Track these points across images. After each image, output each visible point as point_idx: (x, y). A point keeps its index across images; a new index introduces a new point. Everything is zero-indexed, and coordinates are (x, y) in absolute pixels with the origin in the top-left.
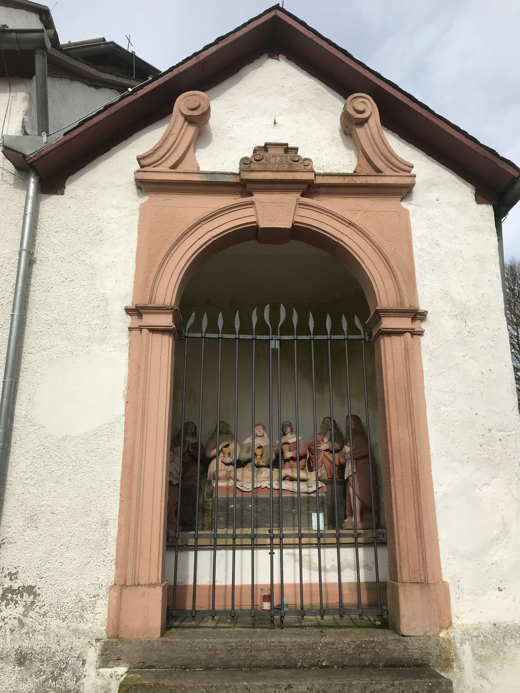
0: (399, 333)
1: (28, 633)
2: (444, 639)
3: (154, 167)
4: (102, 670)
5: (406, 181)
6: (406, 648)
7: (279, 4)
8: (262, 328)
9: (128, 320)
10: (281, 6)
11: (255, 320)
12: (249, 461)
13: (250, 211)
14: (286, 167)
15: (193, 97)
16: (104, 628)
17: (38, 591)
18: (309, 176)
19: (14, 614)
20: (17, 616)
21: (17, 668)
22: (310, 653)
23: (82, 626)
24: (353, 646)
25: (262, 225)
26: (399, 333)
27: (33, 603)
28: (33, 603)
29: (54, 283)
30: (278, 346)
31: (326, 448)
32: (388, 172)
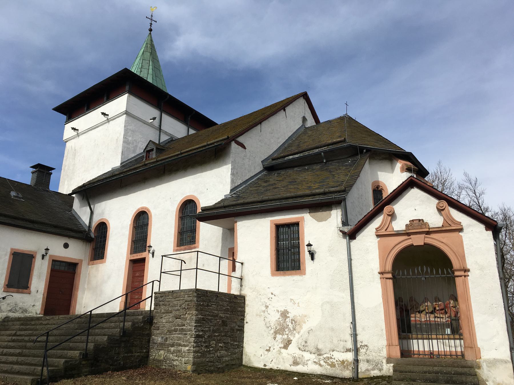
0: (461, 276)
1: (368, 356)
2: (478, 361)
4: (387, 365)
5: (460, 227)
6: (466, 363)
12: (423, 311)
13: (410, 240)
16: (386, 355)
17: (368, 346)
18: (428, 230)
19: (364, 351)
21: (367, 363)
23: (380, 355)
24: (452, 362)
26: (461, 276)
27: (368, 349)
28: (368, 349)
32: (454, 225)
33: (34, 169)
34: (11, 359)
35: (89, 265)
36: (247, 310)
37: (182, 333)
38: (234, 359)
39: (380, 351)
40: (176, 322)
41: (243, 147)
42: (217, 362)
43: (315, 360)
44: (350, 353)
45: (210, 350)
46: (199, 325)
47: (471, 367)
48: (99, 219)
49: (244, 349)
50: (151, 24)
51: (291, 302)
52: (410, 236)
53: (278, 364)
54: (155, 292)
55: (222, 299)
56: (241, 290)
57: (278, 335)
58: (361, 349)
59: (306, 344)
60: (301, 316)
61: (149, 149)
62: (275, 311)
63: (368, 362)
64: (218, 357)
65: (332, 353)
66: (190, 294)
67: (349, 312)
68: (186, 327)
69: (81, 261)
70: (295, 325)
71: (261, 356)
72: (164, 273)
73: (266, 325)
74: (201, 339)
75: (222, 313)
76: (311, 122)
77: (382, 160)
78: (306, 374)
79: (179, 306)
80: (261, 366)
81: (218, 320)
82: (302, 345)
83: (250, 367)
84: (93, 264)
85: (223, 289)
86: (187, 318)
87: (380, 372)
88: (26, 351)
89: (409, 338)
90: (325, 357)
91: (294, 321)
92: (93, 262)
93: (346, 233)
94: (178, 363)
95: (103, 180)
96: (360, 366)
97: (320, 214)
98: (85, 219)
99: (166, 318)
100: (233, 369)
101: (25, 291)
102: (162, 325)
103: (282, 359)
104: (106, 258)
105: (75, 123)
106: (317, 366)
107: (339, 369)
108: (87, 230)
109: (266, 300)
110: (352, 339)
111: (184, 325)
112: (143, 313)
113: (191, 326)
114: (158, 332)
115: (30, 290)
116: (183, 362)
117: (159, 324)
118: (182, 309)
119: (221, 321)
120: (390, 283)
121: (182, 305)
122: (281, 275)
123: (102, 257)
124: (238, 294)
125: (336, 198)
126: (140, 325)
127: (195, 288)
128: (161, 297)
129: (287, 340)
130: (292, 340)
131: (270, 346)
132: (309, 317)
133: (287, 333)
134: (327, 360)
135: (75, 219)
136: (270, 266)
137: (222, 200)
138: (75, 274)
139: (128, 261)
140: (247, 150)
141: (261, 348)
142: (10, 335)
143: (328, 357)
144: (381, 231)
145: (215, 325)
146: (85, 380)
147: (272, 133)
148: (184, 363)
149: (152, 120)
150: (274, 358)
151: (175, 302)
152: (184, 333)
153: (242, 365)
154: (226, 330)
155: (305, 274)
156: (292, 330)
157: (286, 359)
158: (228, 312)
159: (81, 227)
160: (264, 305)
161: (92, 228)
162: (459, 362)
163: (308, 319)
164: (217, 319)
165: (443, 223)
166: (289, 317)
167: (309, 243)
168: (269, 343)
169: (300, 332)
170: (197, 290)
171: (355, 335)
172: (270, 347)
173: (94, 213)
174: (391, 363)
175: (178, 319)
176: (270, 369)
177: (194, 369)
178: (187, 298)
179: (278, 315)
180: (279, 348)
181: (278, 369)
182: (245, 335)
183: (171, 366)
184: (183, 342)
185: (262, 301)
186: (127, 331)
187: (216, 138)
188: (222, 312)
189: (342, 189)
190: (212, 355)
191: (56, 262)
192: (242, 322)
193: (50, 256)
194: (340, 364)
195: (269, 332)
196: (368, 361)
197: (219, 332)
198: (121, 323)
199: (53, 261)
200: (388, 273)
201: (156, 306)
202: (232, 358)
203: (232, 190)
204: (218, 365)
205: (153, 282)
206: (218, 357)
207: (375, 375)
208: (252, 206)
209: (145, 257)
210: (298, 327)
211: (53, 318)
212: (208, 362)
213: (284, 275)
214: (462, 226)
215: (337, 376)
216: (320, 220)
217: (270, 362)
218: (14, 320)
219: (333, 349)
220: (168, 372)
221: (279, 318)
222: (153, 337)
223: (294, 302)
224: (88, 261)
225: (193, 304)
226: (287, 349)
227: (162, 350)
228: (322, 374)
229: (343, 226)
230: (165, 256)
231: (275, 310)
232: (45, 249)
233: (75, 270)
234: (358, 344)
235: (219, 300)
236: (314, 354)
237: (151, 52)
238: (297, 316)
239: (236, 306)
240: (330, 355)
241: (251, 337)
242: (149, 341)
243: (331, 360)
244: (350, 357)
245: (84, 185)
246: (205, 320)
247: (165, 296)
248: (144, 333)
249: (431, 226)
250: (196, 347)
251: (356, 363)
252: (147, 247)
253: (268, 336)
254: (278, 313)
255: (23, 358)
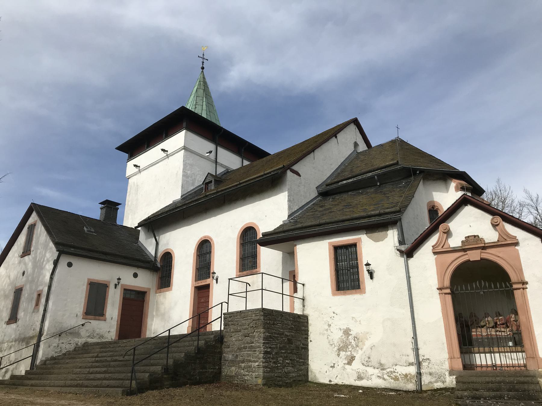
0: (519, 289)
2: (540, 371)
12: (485, 326)
13: (467, 256)
14: (475, 243)
16: (448, 368)
17: (430, 360)
18: (483, 245)
22: (503, 374)
23: (443, 367)
24: (514, 372)
26: (519, 289)
27: (430, 362)
28: (430, 362)
31: (513, 320)
32: (509, 240)
33: (103, 205)
34: (98, 376)
35: (156, 293)
36: (311, 329)
37: (251, 350)
38: (300, 376)
39: (442, 364)
40: (245, 340)
41: (299, 175)
42: (285, 377)
43: (378, 375)
44: (413, 366)
45: (278, 366)
46: (267, 342)
47: (534, 376)
48: (164, 249)
49: (309, 367)
50: (203, 62)
51: (353, 320)
52: (467, 252)
53: (343, 380)
54: (223, 313)
55: (287, 318)
56: (303, 310)
57: (341, 352)
58: (423, 363)
59: (370, 360)
60: (363, 333)
61: (207, 181)
62: (338, 329)
63: (431, 375)
64: (285, 373)
66: (257, 313)
68: (255, 344)
69: (149, 289)
70: (358, 342)
71: (326, 372)
72: (231, 295)
73: (329, 342)
74: (269, 355)
75: (287, 332)
76: (362, 147)
77: (436, 180)
78: (370, 388)
79: (247, 325)
80: (327, 382)
81: (284, 338)
82: (366, 360)
83: (316, 383)
84: (160, 293)
85: (287, 309)
86: (255, 336)
87: (443, 384)
88: (112, 369)
89: (471, 353)
90: (388, 371)
91: (357, 338)
92: (161, 290)
93: (403, 251)
94: (249, 377)
95: (167, 212)
96: (423, 379)
97: (376, 235)
98: (151, 249)
99: (235, 336)
100: (300, 384)
101: (101, 318)
102: (233, 344)
103: (346, 375)
104: (172, 286)
105: (136, 161)
106: (381, 380)
107: (402, 382)
108: (153, 260)
109: (329, 319)
110: (414, 353)
111: (253, 343)
112: (214, 333)
113: (260, 343)
114: (228, 350)
115: (105, 317)
116: (254, 377)
117: (230, 342)
118: (250, 328)
119: (286, 339)
120: (449, 298)
121: (250, 324)
122: (341, 294)
123: (168, 285)
124: (302, 314)
125: (391, 219)
126: (212, 343)
127: (261, 307)
128: (230, 317)
129: (350, 357)
130: (355, 357)
131: (334, 362)
132: (371, 334)
133: (350, 350)
134: (390, 374)
135: (141, 250)
136: (330, 286)
137: (281, 226)
138: (144, 301)
139: (194, 288)
140: (301, 177)
141: (325, 364)
142: (92, 357)
143: (391, 371)
144: (438, 248)
145: (282, 343)
146: (168, 391)
147: (325, 160)
148: (255, 378)
149: (209, 154)
150: (339, 374)
151: (244, 321)
152: (253, 349)
153: (308, 381)
154: (292, 348)
155: (365, 293)
156: (355, 347)
157: (351, 374)
158: (293, 331)
159: (148, 258)
160: (327, 324)
161: (158, 258)
162: (522, 372)
163: (370, 336)
164: (283, 337)
165: (499, 238)
166: (351, 335)
167: (368, 263)
168: (333, 360)
169: (363, 348)
170: (263, 310)
171: (416, 350)
172: (334, 364)
173: (159, 244)
174: (454, 375)
175: (247, 337)
176: (335, 384)
177: (265, 383)
178: (255, 317)
179: (341, 333)
180: (344, 365)
181: (343, 384)
182: (310, 353)
183: (243, 381)
184: (253, 358)
185: (324, 320)
186: (201, 349)
187: (272, 168)
188: (287, 331)
189: (398, 209)
190: (280, 371)
191: (127, 291)
192: (306, 340)
193: (122, 285)
194: (404, 377)
195: (333, 349)
196: (430, 374)
197: (285, 350)
198: (194, 342)
199: (125, 290)
200: (447, 288)
201: (225, 326)
202: (298, 375)
203: (289, 216)
204: (286, 381)
205: (222, 303)
206: (285, 373)
207: (438, 387)
208: (310, 229)
209: (210, 284)
210: (360, 344)
211: (130, 341)
212: (276, 377)
213: (344, 294)
214: (518, 240)
215: (401, 389)
216: (376, 240)
217: (335, 378)
218: (93, 344)
219: (395, 364)
220: (241, 386)
221: (342, 336)
222: (224, 354)
223: (356, 320)
224: (156, 289)
225: (260, 323)
226: (351, 365)
227: (233, 366)
228: (386, 387)
229: (400, 245)
230: (231, 279)
231: (338, 328)
232: (117, 279)
233: (144, 299)
234: (420, 358)
235: (284, 319)
236: (377, 368)
237: (204, 89)
238: (359, 333)
239: (300, 325)
240: (394, 369)
241: (316, 355)
242: (220, 359)
243: (395, 374)
244: (413, 370)
245: (149, 218)
246: (272, 338)
247: (234, 316)
248: (216, 350)
249: (487, 241)
250: (265, 362)
251: (419, 376)
252: (211, 274)
253: (332, 353)
254: (341, 330)
255: (110, 375)
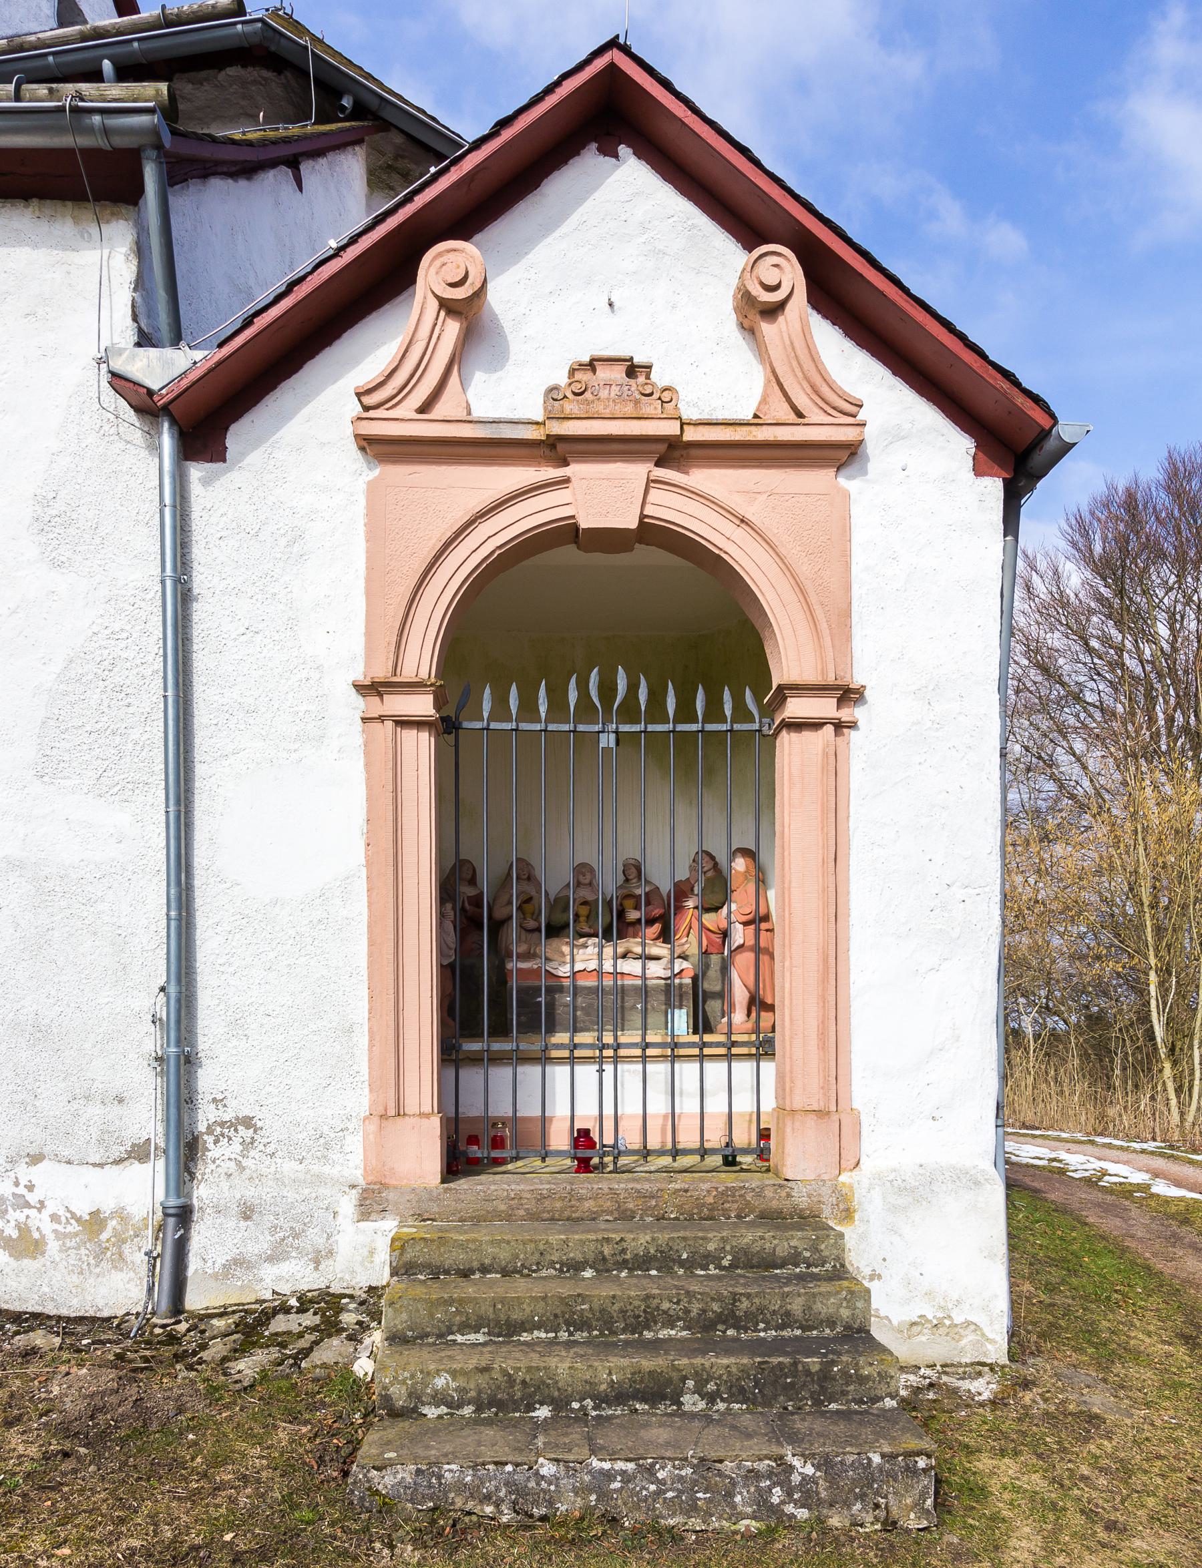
0: (815, 725)
3: (387, 409)
4: (362, 1224)
6: (789, 1195)
7: (617, 36)
8: (586, 709)
9: (359, 704)
10: (621, 41)
11: (573, 696)
15: (451, 256)
16: (359, 1173)
17: (259, 1124)
18: (671, 428)
20: (233, 1156)
22: (653, 1203)
23: (327, 1169)
24: (715, 1193)
25: (584, 524)
26: (815, 725)
29: (226, 636)
30: (612, 744)
39: (325, 1144)
47: (807, 1219)
52: (565, 463)
58: (211, 1146)
63: (247, 1218)
65: (25, 1173)
67: (153, 928)
87: (316, 1269)
162: (753, 1190)
165: (764, 400)
194: (76, 1234)
196: (247, 1213)
240: (17, 1184)
